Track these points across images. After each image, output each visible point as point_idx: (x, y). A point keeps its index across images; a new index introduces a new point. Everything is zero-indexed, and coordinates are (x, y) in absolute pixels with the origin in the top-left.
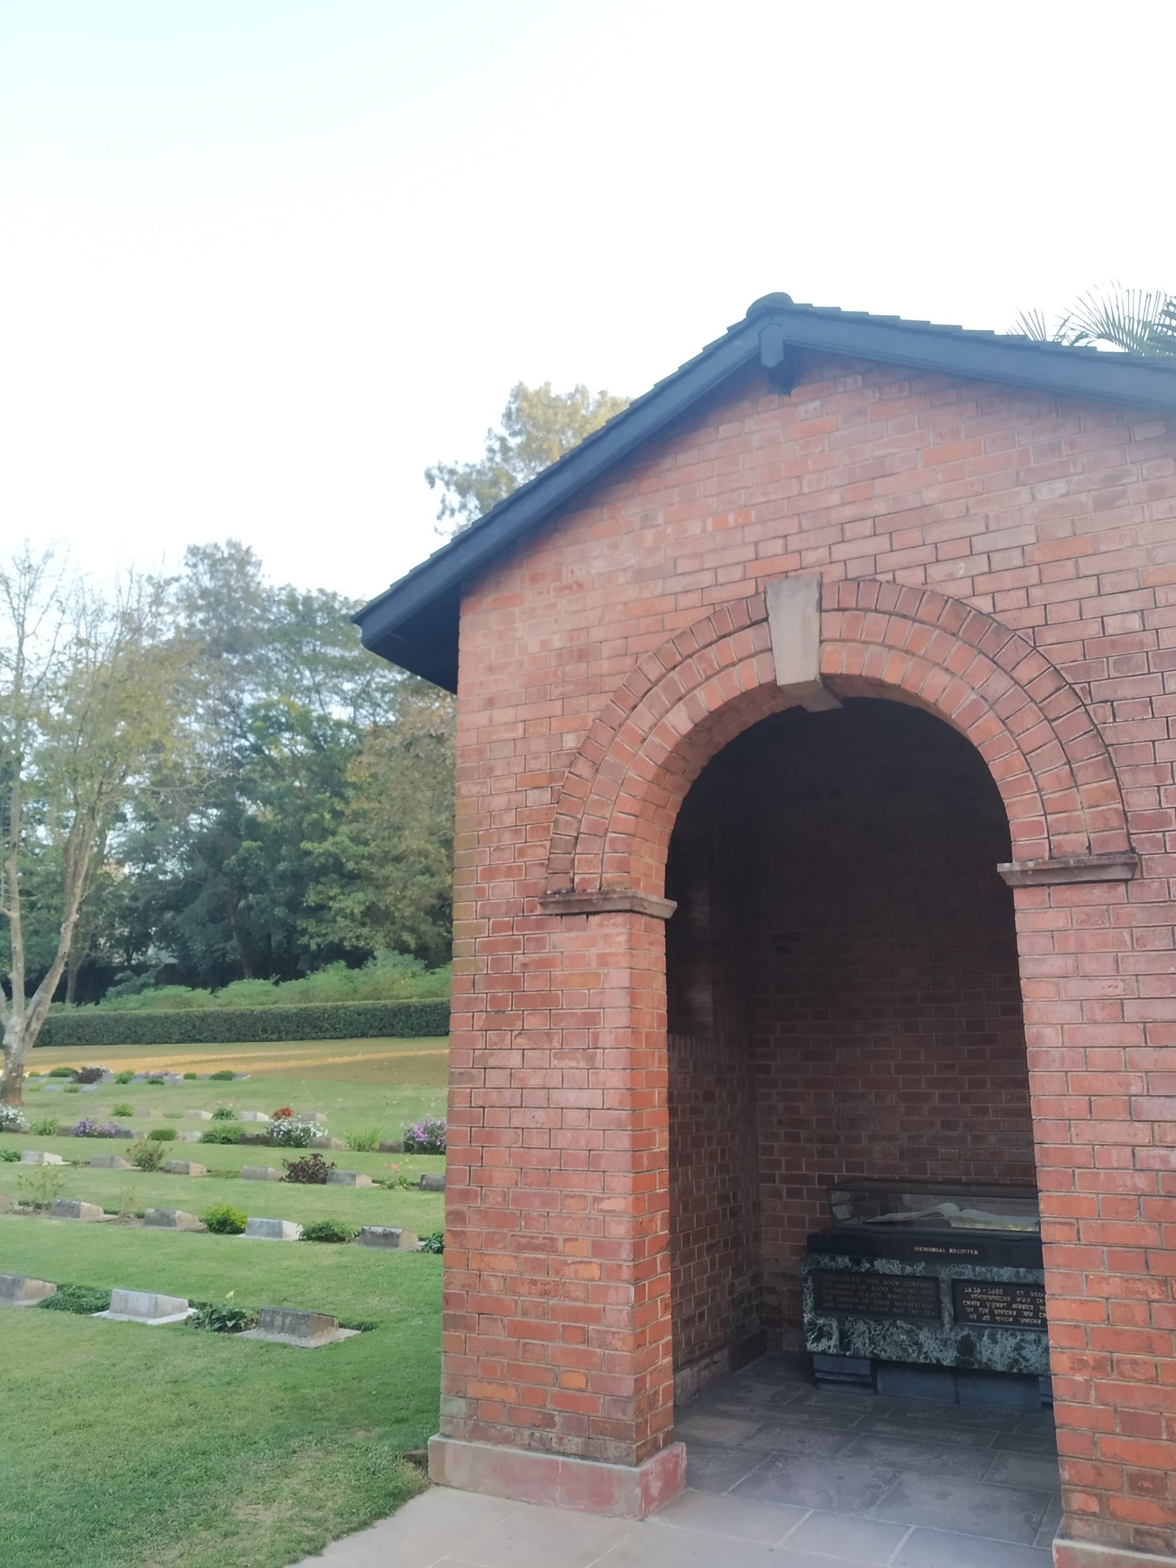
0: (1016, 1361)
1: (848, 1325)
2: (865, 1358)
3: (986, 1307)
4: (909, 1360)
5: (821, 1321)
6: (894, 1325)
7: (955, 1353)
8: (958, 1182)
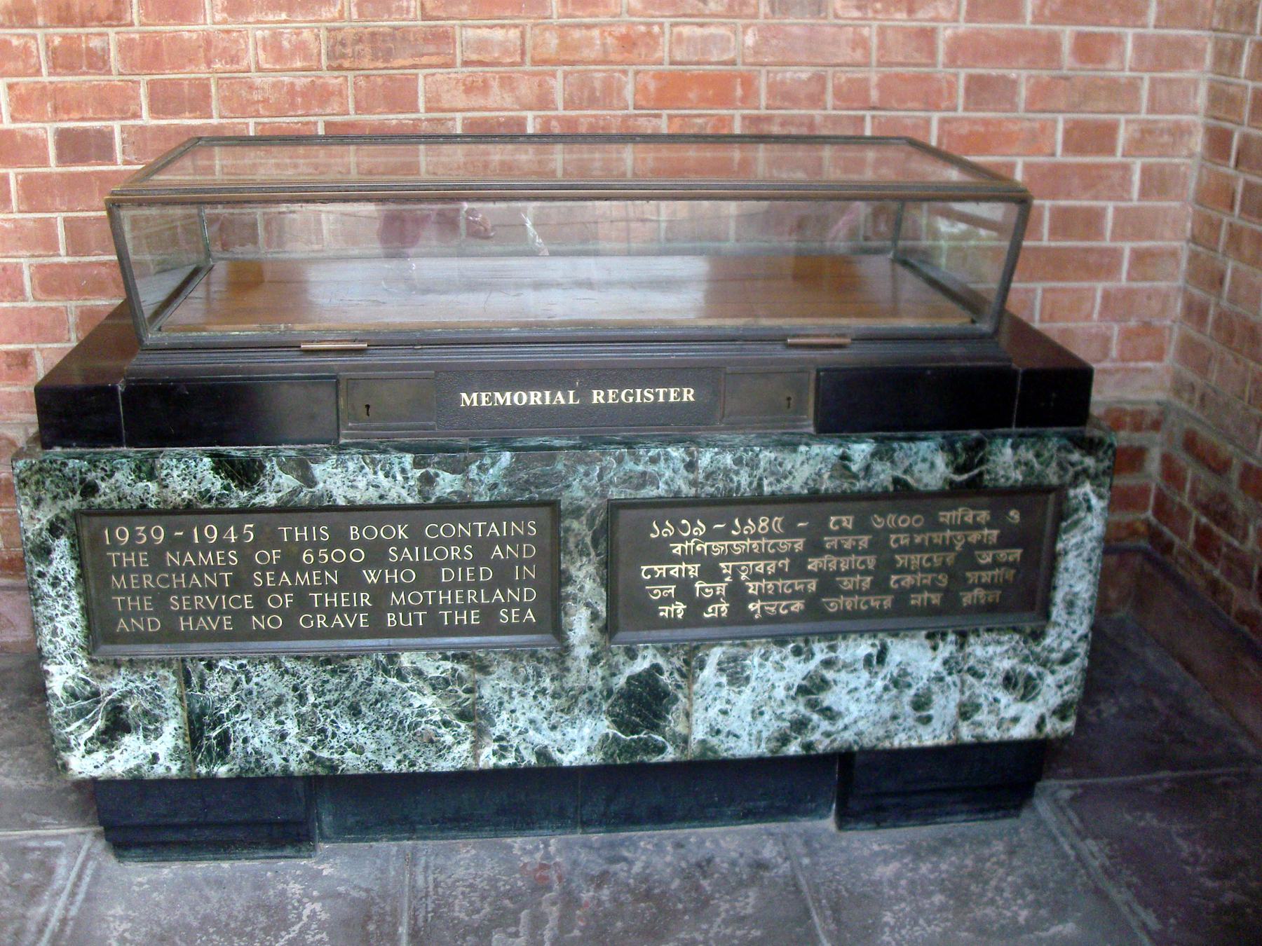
0: (800, 725)
1: (218, 685)
3: (719, 577)
4: (444, 765)
5: (117, 684)
6: (389, 666)
7: (605, 726)
8: (513, 135)
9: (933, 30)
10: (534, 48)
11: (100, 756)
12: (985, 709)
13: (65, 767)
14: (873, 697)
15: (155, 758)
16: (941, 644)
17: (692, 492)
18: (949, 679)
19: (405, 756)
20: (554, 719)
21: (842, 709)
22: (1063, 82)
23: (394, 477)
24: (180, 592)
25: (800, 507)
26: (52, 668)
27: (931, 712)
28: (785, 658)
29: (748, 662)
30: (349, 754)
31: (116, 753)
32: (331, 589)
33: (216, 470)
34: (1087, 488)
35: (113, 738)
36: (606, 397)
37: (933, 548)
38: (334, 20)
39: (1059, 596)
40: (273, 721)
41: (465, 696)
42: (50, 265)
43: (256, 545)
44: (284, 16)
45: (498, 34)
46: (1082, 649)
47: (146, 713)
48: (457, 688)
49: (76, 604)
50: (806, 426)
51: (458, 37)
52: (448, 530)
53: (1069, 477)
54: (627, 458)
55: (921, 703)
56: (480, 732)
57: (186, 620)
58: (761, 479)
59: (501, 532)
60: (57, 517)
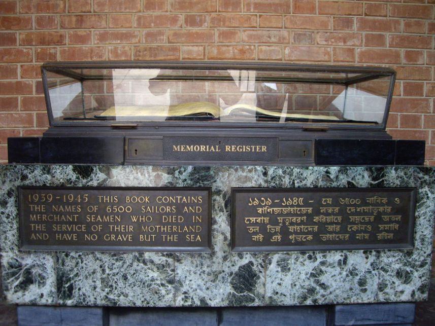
0: (312, 291)
1: (70, 264)
2: (96, 306)
3: (277, 224)
4: (161, 304)
5: (28, 261)
6: (140, 258)
7: (229, 289)
9: (353, 49)
10: (208, 53)
11: (20, 294)
12: (389, 286)
13: (5, 298)
14: (342, 279)
15: (42, 295)
16: (370, 256)
17: (266, 185)
18: (373, 272)
19: (145, 299)
20: (208, 284)
21: (329, 284)
22: (402, 69)
23: (144, 175)
24: (57, 223)
25: (310, 194)
26: (4, 254)
27: (366, 287)
28: (305, 260)
29: (289, 262)
30: (122, 297)
31: (26, 293)
32: (117, 223)
33: (74, 170)
34: (426, 189)
35: (26, 286)
36: (231, 149)
37: (365, 213)
38: (136, 43)
39: (418, 236)
40: (91, 281)
41: (171, 273)
42: (30, 130)
43: (89, 203)
44: (119, 42)
45: (195, 49)
46: (429, 260)
47: (40, 275)
48: (167, 269)
49: (15, 226)
50: (311, 161)
51: (181, 48)
52: (166, 199)
53: (418, 184)
54: (239, 170)
55: (362, 283)
56: (177, 289)
57: (59, 235)
58: (294, 180)
59: (187, 201)
60: (11, 188)
